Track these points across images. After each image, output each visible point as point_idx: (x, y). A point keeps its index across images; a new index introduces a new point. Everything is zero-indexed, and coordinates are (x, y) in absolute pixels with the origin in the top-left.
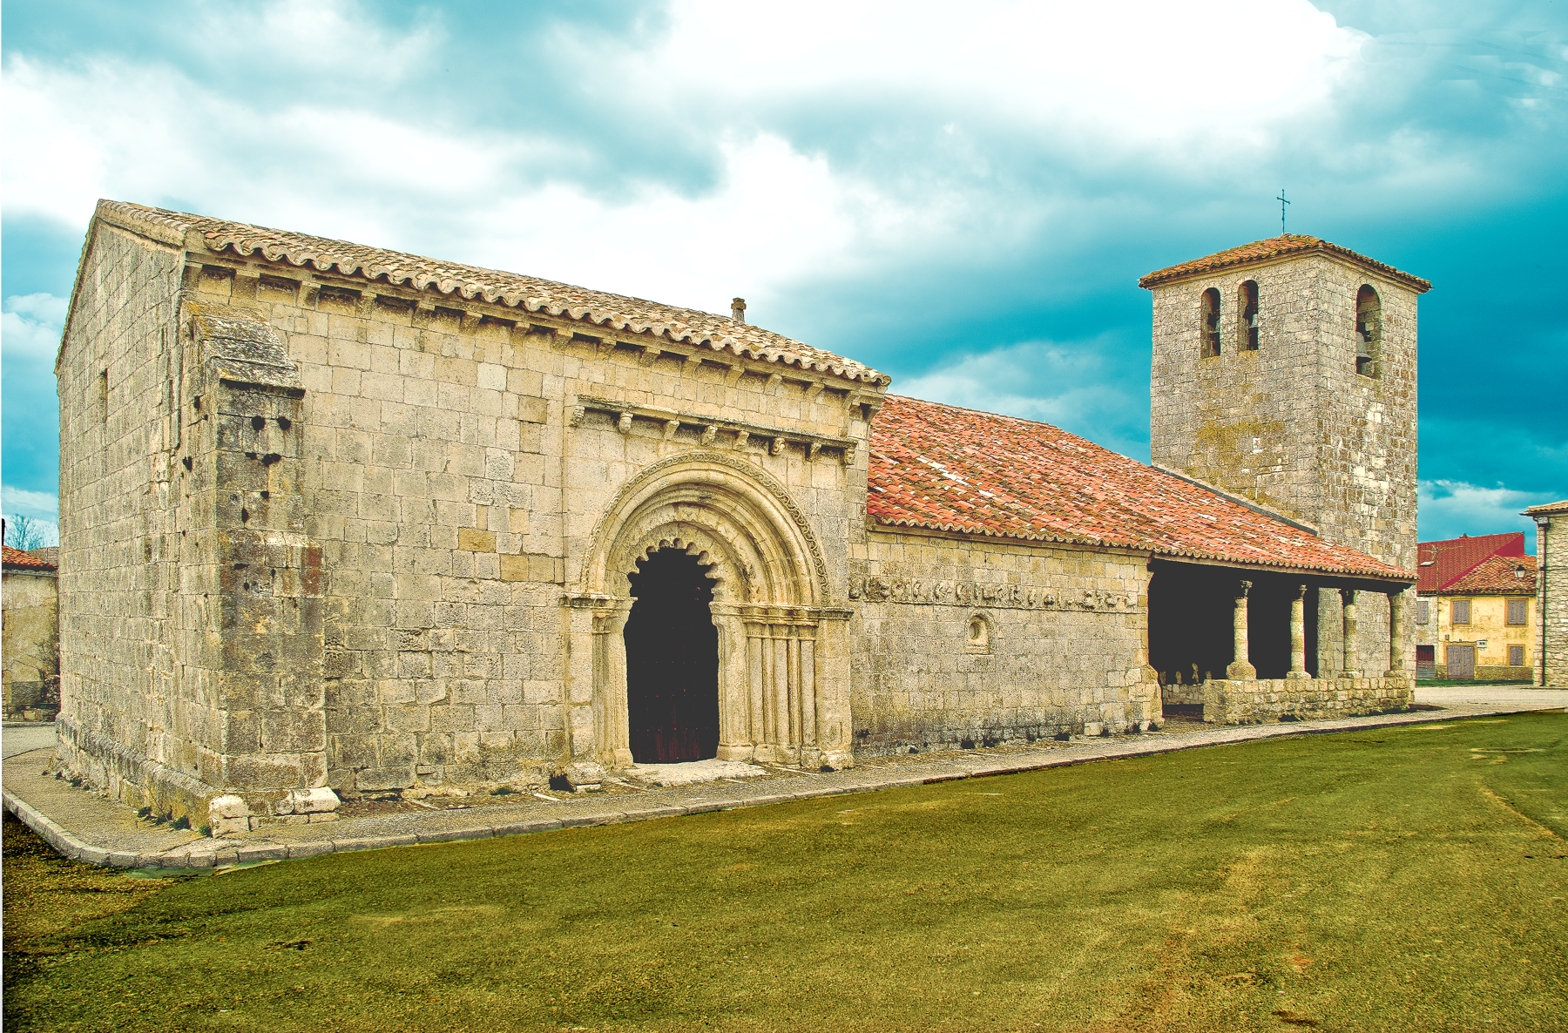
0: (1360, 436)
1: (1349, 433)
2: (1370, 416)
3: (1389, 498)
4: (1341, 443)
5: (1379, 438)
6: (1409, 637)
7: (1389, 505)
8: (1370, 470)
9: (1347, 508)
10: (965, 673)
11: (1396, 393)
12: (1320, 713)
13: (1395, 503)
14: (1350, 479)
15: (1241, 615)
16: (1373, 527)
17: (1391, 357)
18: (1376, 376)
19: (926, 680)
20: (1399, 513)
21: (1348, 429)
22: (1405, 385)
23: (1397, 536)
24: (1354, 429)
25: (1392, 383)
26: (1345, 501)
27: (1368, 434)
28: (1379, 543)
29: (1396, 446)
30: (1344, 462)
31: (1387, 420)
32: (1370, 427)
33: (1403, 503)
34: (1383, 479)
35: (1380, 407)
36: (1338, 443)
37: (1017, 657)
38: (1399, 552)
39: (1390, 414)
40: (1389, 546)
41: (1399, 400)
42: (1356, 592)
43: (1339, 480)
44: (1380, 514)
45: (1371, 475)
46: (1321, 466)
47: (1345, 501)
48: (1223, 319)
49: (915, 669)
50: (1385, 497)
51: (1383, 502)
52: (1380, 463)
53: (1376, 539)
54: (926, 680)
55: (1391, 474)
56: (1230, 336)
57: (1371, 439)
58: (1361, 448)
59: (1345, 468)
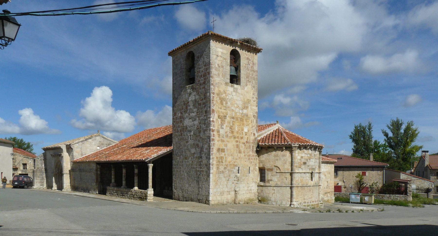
3: (198, 126)
4: (180, 114)
8: (190, 118)
12: (124, 197)
14: (183, 125)
15: (113, 172)
16: (192, 139)
24: (184, 107)
28: (194, 144)
33: (204, 126)
34: (195, 120)
36: (179, 114)
38: (201, 146)
40: (198, 145)
44: (194, 133)
45: (191, 120)
51: (196, 128)
53: (193, 143)
55: (199, 117)
58: (187, 112)
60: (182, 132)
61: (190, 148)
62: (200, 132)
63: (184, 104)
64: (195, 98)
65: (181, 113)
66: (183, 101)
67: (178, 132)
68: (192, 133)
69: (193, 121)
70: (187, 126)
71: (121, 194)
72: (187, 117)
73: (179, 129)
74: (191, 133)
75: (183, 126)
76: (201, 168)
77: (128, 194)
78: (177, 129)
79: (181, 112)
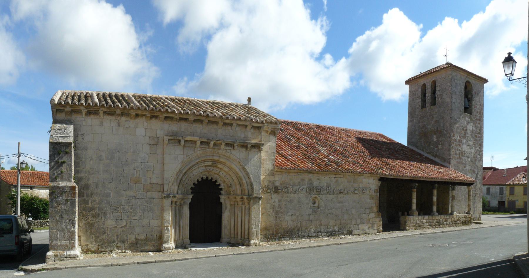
0: (465, 134)
1: (461, 133)
2: (468, 128)
3: (474, 155)
4: (458, 137)
5: (471, 135)
6: (480, 200)
7: (474, 157)
8: (468, 146)
9: (460, 158)
10: (309, 215)
11: (477, 119)
13: (476, 156)
14: (461, 149)
15: (414, 195)
16: (469, 164)
17: (476, 107)
18: (471, 113)
19: (294, 217)
20: (477, 160)
21: (461, 132)
22: (480, 117)
23: (476, 167)
24: (463, 132)
25: (476, 116)
26: (460, 156)
27: (467, 133)
28: (471, 170)
29: (476, 137)
30: (459, 143)
31: (474, 129)
32: (468, 131)
33: (479, 156)
34: (472, 148)
35: (472, 124)
36: (458, 137)
37: (328, 210)
38: (477, 173)
39: (475, 126)
40: (474, 171)
41: (478, 122)
42: (455, 186)
43: (458, 149)
44: (471, 160)
45: (468, 147)
46: (452, 145)
47: (460, 156)
48: (427, 95)
49: (290, 214)
50: (473, 155)
51: (472, 156)
52: (471, 143)
53: (470, 169)
54: (294, 217)
55: (475, 147)
56: (429, 100)
57: (469, 135)
58: (465, 138)
59: (460, 145)
60: (461, 156)
61: (467, 172)
62: (476, 160)
63: (463, 129)
64: (472, 129)
65: (460, 137)
66: (462, 126)
67: (456, 154)
68: (469, 160)
69: (470, 149)
70: (465, 152)
71: (437, 224)
72: (465, 143)
73: (458, 152)
74: (469, 160)
75: (462, 151)
76: (476, 191)
77: (448, 221)
78: (456, 152)
79: (460, 136)
